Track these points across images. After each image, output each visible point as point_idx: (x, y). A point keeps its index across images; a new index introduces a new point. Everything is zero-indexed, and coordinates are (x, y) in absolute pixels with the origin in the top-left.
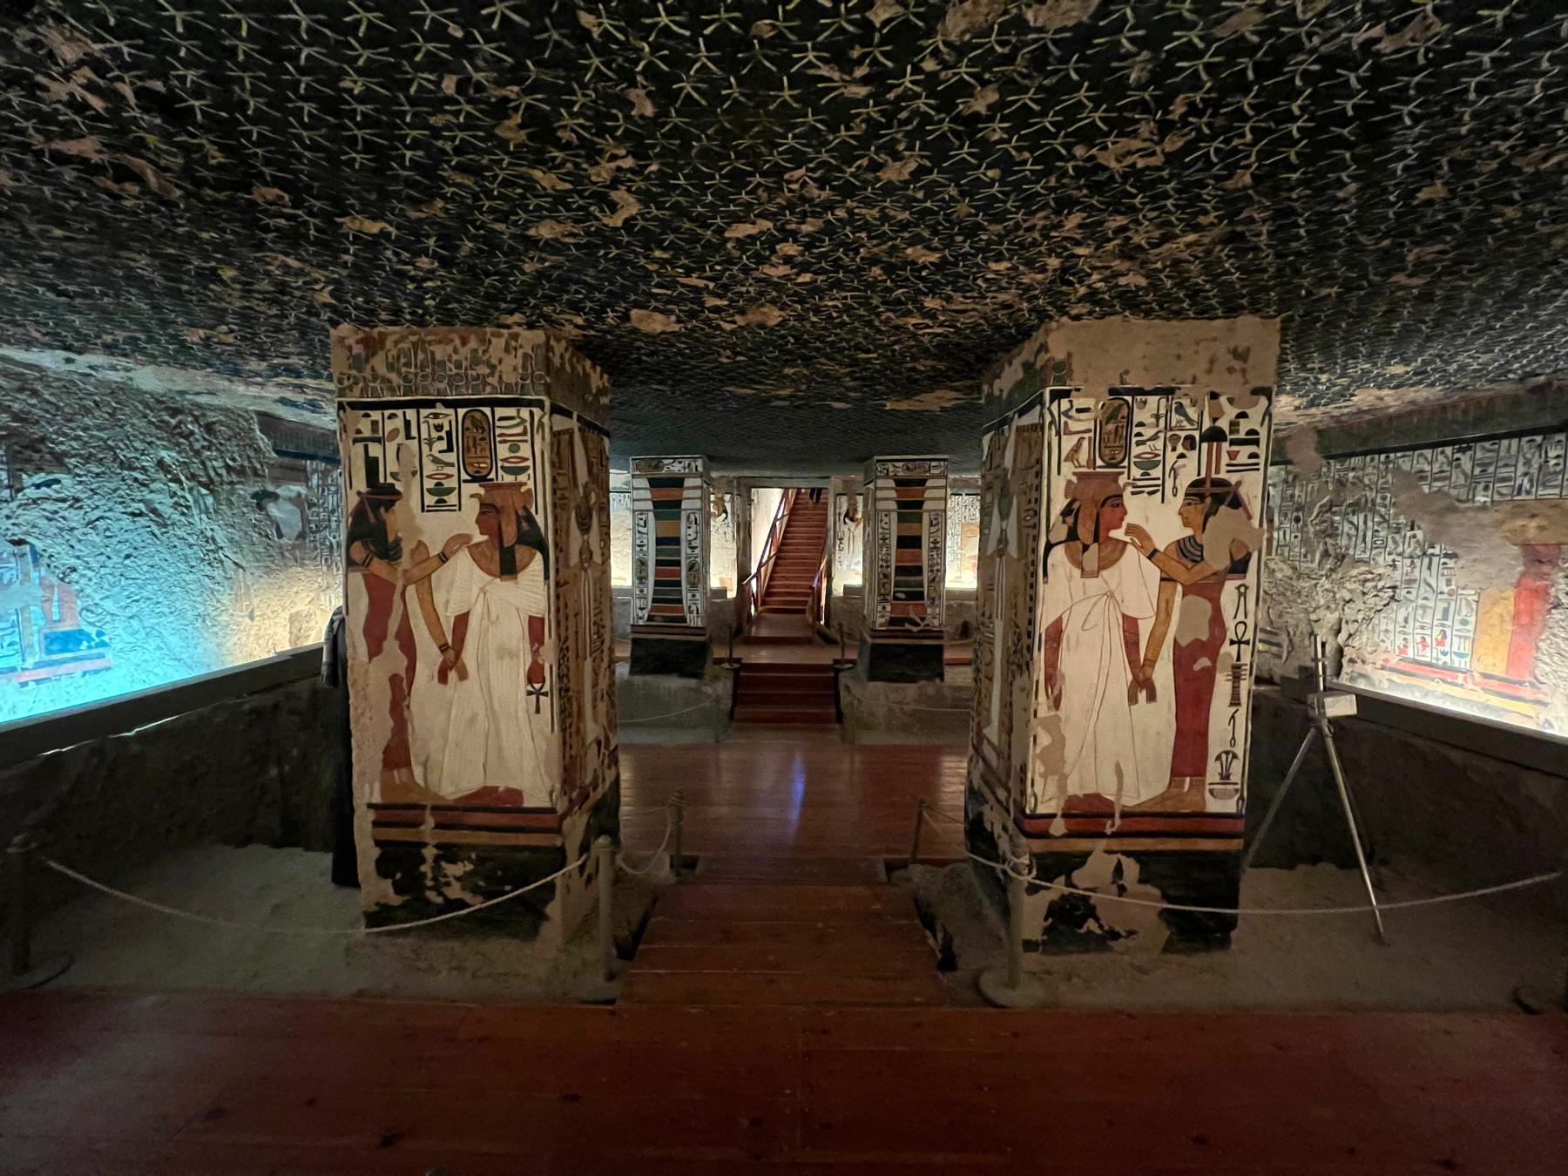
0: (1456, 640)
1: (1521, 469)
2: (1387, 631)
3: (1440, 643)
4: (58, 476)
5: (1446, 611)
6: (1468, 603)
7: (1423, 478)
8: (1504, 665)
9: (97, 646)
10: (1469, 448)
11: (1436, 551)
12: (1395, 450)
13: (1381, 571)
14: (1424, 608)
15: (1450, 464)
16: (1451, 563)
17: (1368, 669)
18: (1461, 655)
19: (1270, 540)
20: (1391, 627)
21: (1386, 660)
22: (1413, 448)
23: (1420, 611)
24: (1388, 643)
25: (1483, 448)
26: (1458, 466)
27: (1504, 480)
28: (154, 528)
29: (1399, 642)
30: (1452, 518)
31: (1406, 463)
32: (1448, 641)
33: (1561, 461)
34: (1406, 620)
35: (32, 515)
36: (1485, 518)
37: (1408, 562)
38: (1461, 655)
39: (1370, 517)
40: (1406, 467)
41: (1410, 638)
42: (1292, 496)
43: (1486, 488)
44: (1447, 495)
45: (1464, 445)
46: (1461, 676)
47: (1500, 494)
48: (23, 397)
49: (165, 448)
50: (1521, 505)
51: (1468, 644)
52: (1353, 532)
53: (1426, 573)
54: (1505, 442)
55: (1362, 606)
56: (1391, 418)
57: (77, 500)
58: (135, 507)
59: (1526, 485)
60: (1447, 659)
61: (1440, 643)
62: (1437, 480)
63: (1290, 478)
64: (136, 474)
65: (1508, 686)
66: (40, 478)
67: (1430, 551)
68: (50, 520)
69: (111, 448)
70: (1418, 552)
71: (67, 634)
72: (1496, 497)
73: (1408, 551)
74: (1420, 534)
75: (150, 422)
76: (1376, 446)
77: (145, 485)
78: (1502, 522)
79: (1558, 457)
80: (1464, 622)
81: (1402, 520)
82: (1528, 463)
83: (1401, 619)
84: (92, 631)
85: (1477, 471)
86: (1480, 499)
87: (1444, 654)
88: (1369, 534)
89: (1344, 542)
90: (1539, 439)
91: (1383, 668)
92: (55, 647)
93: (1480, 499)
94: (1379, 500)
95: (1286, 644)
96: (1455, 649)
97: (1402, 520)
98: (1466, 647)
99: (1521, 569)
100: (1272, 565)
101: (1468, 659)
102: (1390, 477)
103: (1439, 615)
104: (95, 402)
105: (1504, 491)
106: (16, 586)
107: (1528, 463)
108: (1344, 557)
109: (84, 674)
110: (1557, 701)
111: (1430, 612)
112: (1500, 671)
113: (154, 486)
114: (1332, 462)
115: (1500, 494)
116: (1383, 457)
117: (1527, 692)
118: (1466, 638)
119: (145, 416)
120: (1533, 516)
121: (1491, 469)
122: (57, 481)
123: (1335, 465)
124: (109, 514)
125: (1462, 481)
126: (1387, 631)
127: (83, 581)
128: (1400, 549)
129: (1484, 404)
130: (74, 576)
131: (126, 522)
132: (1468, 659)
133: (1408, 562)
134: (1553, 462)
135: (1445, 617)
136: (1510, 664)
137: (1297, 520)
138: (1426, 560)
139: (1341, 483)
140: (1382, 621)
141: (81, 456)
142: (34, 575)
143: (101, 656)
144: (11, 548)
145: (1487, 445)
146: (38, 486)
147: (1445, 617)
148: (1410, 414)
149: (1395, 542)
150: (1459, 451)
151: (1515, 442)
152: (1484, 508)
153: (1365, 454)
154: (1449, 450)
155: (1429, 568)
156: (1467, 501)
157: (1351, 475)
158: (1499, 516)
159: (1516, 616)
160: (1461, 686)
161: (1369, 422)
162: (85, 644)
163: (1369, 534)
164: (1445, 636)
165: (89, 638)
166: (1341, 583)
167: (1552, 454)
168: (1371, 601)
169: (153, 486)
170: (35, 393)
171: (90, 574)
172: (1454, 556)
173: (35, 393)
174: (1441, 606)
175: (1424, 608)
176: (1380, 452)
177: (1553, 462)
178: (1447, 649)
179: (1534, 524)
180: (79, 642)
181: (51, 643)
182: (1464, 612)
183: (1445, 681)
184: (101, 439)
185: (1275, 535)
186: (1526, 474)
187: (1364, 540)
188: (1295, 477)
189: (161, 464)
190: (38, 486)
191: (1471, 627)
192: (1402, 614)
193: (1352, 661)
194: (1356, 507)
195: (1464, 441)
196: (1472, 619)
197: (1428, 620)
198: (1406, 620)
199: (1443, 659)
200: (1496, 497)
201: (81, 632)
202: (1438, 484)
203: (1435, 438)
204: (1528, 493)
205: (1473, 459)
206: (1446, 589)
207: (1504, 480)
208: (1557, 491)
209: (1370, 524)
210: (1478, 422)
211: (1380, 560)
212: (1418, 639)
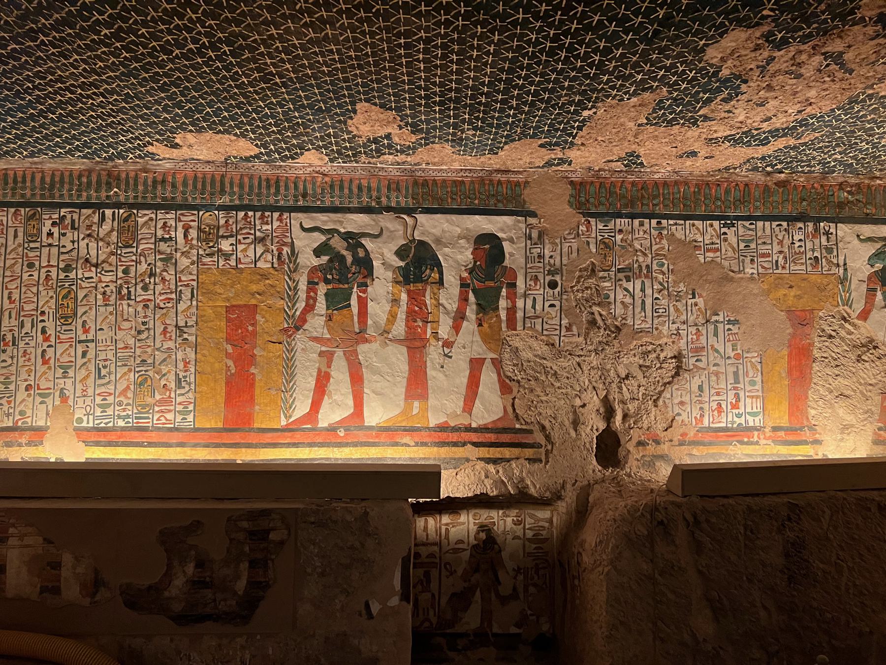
0: (748, 400)
2: (682, 403)
3: (735, 406)
5: (736, 374)
6: (753, 366)
7: (697, 248)
8: (787, 417)
12: (668, 217)
13: (663, 341)
14: (717, 374)
15: (719, 237)
16: (735, 329)
17: (665, 448)
19: (512, 311)
20: (686, 399)
21: (684, 435)
22: (686, 218)
23: (714, 378)
24: (684, 416)
25: (744, 226)
26: (726, 240)
27: (763, 255)
29: (696, 413)
30: (728, 288)
31: (680, 230)
32: (741, 404)
33: (802, 244)
34: (700, 388)
36: (755, 288)
37: (693, 330)
39: (648, 283)
40: (680, 235)
41: (706, 406)
42: (541, 256)
43: (752, 260)
45: (728, 221)
46: (756, 433)
47: (763, 267)
50: (780, 277)
51: (759, 403)
52: (628, 300)
53: (712, 340)
54: (760, 224)
55: (643, 382)
56: (656, 183)
59: (781, 261)
61: (735, 406)
62: (709, 250)
63: (535, 234)
65: (792, 433)
67: (714, 318)
70: (701, 320)
73: (691, 319)
74: (700, 301)
76: (646, 209)
78: (769, 291)
79: (800, 240)
80: (753, 383)
81: (682, 287)
82: (781, 243)
83: (695, 388)
85: (742, 245)
86: (749, 270)
87: (739, 416)
88: (649, 302)
89: (620, 311)
90: (785, 224)
91: (681, 444)
93: (749, 270)
94: (655, 267)
95: (543, 441)
96: (749, 410)
97: (682, 287)
98: (757, 406)
99: (790, 331)
100: (516, 343)
101: (761, 417)
102: (664, 242)
105: (765, 265)
107: (781, 243)
108: (618, 329)
110: (826, 438)
111: (722, 377)
112: (784, 422)
114: (593, 221)
115: (763, 267)
116: (654, 222)
117: (807, 435)
118: (757, 397)
120: (791, 287)
121: (753, 246)
123: (597, 225)
125: (730, 253)
126: (682, 403)
128: (684, 317)
129: (742, 187)
132: (761, 417)
133: (693, 330)
134: (797, 244)
135: (737, 381)
136: (791, 415)
137: (553, 285)
138: (711, 327)
139: (606, 246)
140: (674, 395)
145: (747, 224)
147: (737, 381)
148: (676, 183)
149: (677, 310)
151: (767, 224)
152: (752, 279)
153: (632, 216)
154: (716, 224)
155: (716, 334)
156: (740, 272)
157: (619, 237)
159: (790, 372)
160: (757, 443)
161: (633, 184)
163: (649, 302)
166: (617, 356)
167: (796, 238)
168: (655, 374)
172: (735, 322)
175: (717, 374)
176: (650, 216)
177: (797, 244)
178: (742, 410)
179: (793, 292)
182: (751, 374)
183: (742, 443)
185: (520, 303)
186: (780, 252)
187: (643, 309)
188: (541, 235)
191: (758, 386)
192: (696, 382)
193: (640, 444)
194: (628, 273)
196: (758, 379)
197: (723, 386)
198: (700, 388)
203: (701, 211)
204: (783, 268)
205: (737, 234)
206: (732, 355)
207: (763, 255)
208: (804, 267)
209: (649, 291)
210: (741, 201)
211: (665, 330)
212: (714, 405)
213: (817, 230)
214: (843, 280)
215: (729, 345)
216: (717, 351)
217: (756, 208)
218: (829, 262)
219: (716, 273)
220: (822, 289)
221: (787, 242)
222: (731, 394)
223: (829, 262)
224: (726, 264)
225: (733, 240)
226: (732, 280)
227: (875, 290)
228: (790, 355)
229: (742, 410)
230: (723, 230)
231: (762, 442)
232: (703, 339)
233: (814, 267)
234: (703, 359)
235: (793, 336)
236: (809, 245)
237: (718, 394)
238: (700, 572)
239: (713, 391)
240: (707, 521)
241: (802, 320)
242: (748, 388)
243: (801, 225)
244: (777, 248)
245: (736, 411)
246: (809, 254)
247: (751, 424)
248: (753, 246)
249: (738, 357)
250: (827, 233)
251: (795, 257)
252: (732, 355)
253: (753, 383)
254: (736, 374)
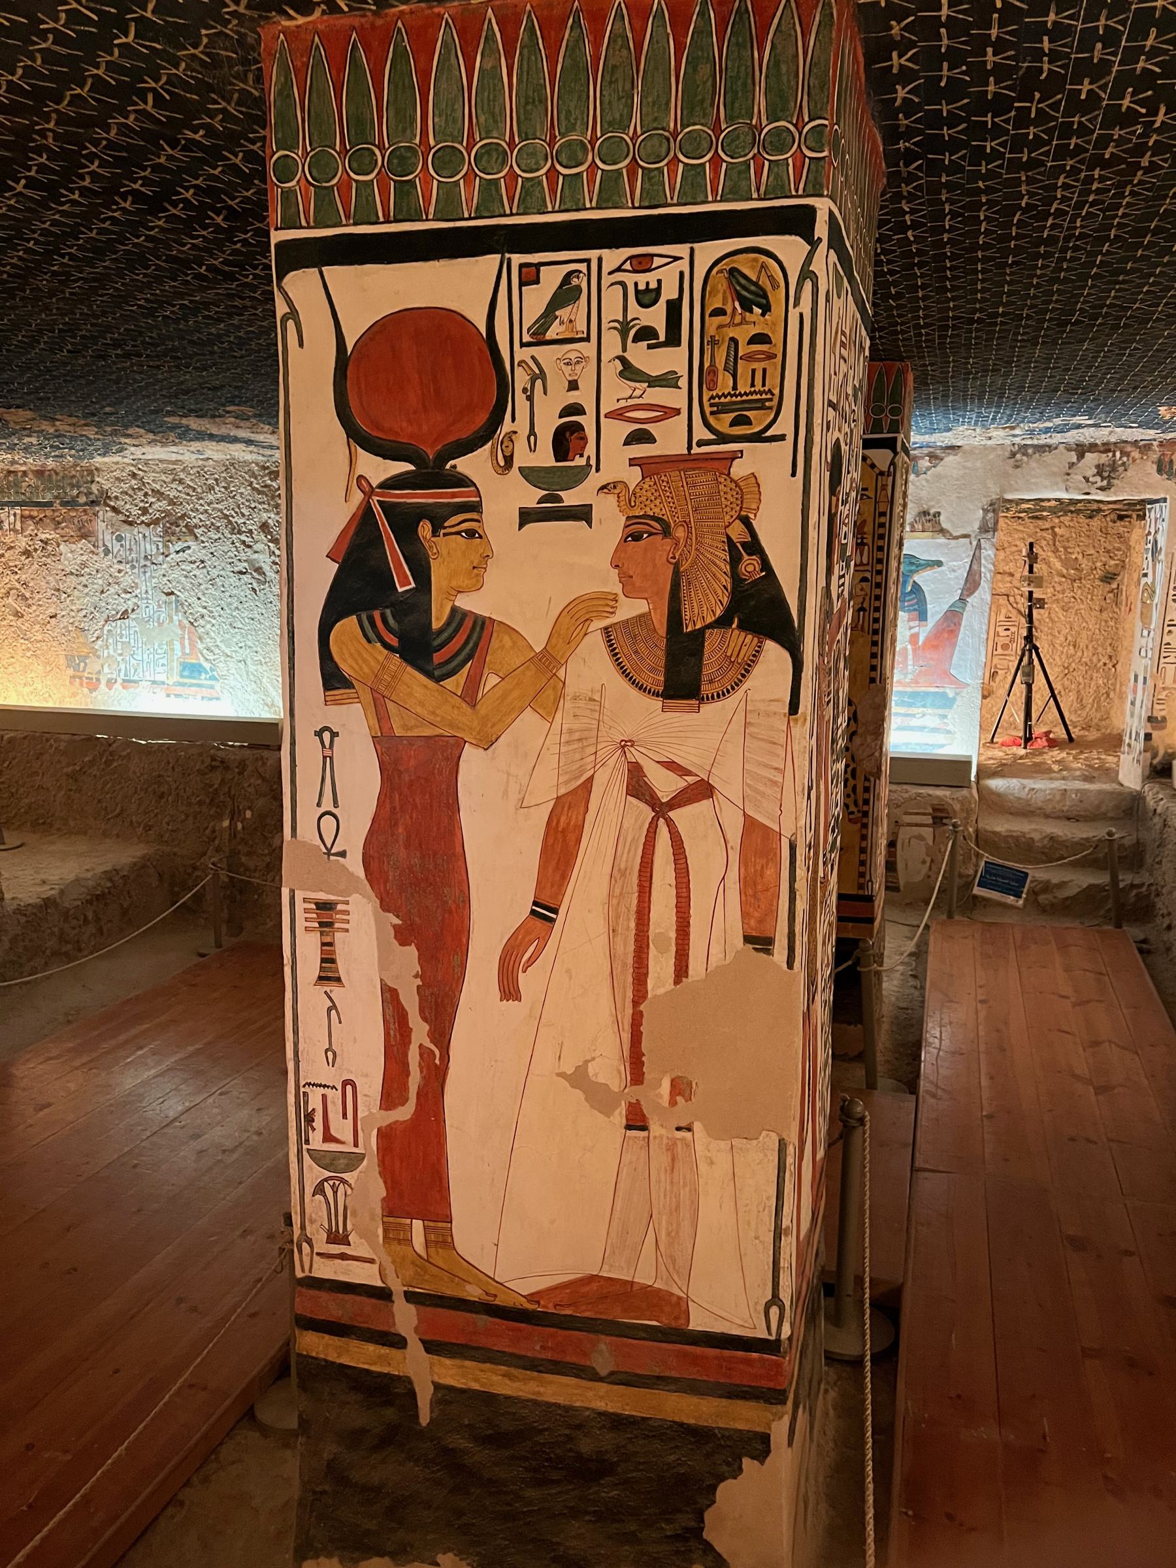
4: (190, 543)
9: (210, 679)
28: (255, 585)
35: (176, 574)
48: (173, 486)
49: (267, 511)
57: (202, 562)
58: (241, 566)
64: (243, 537)
66: (179, 545)
68: (186, 577)
69: (226, 517)
71: (193, 665)
75: (254, 489)
77: (249, 547)
84: (207, 666)
92: (186, 673)
104: (216, 480)
106: (166, 624)
109: (203, 698)
113: (257, 547)
119: (251, 484)
122: (189, 547)
124: (222, 573)
127: (209, 626)
130: (201, 622)
131: (233, 579)
141: (205, 526)
142: (175, 618)
143: (212, 687)
144: (164, 597)
146: (178, 552)
162: (203, 676)
165: (206, 673)
169: (255, 547)
170: (181, 482)
171: (214, 622)
173: (181, 482)
180: (200, 673)
181: (184, 669)
184: (221, 511)
189: (264, 527)
190: (178, 552)
201: (200, 665)
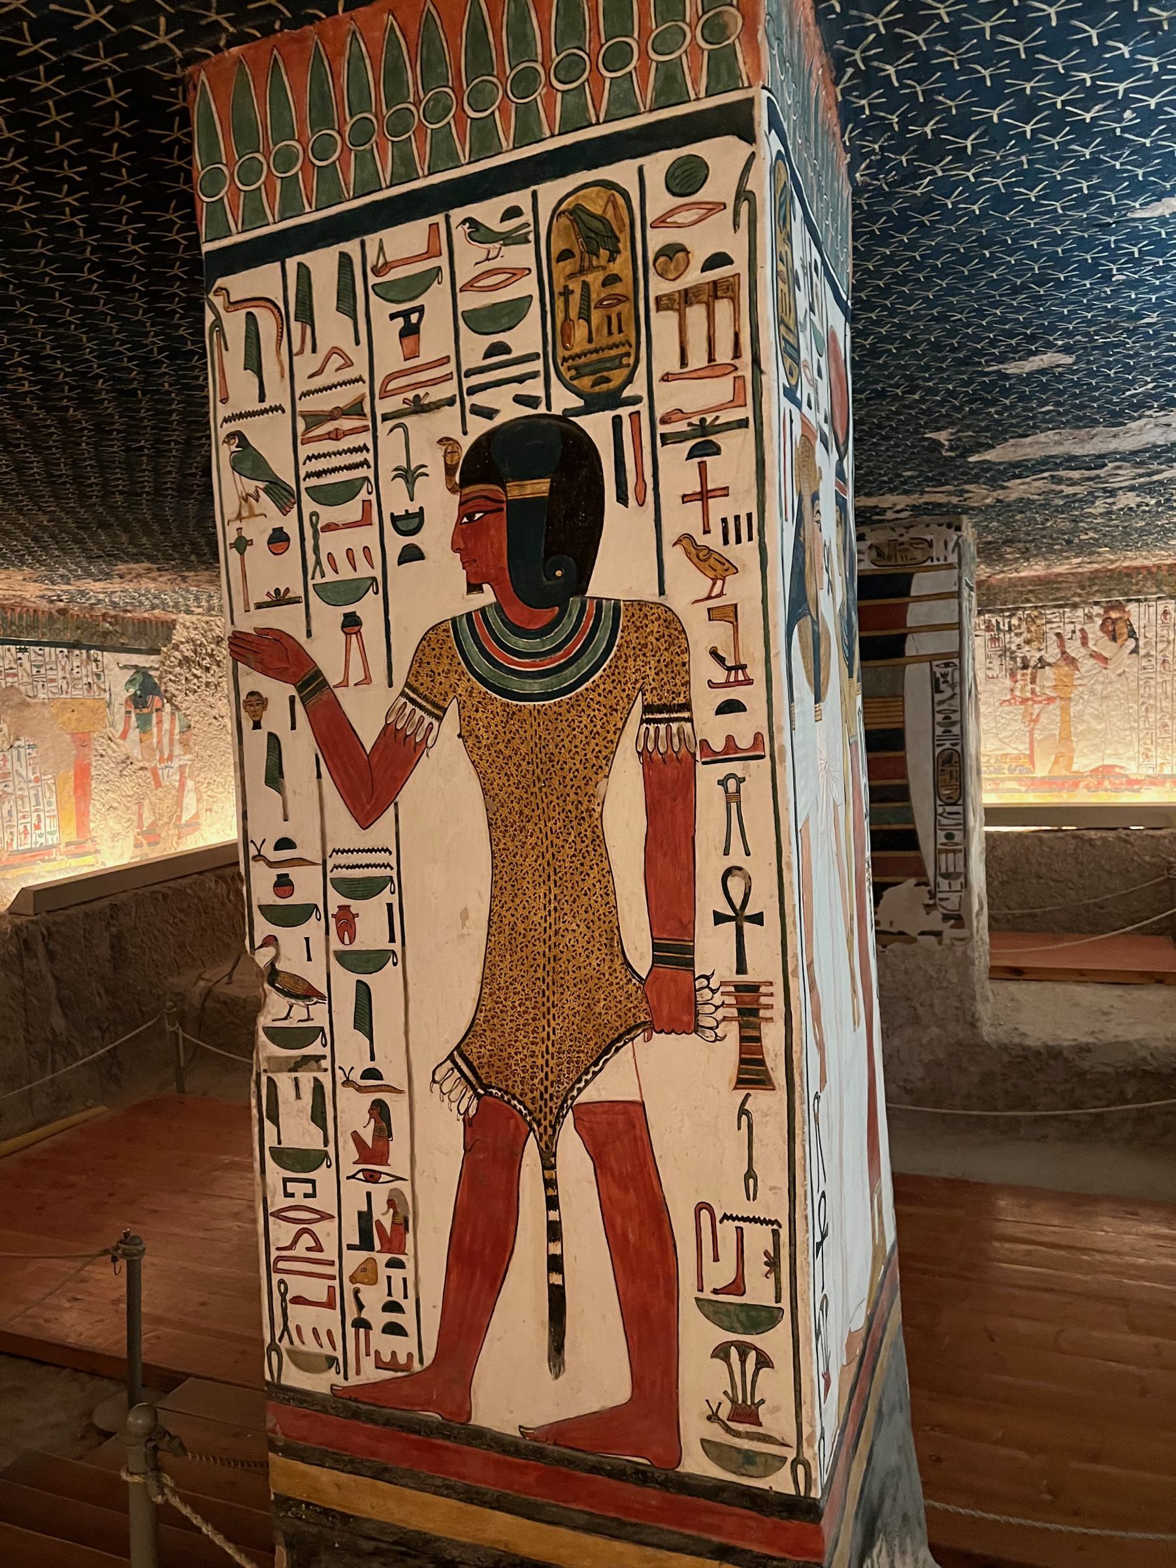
1: (61, 674)
3: (37, 827)
5: (36, 796)
6: (49, 787)
10: (26, 650)
11: (21, 743)
14: (22, 797)
18: (52, 833)
23: (20, 802)
26: (21, 665)
30: (27, 713)
32: (42, 824)
38: (52, 833)
44: (18, 690)
45: (23, 646)
53: (17, 765)
54: (47, 649)
60: (42, 840)
67: (17, 743)
72: (51, 696)
82: (63, 668)
85: (34, 670)
86: (41, 696)
87: (40, 836)
90: (65, 650)
96: (48, 829)
99: (74, 752)
103: (33, 803)
105: (54, 690)
107: (63, 668)
111: (26, 800)
125: (26, 679)
135: (38, 804)
138: (15, 752)
145: (37, 649)
147: (38, 804)
150: (20, 650)
155: (19, 760)
156: (35, 697)
158: (54, 710)
160: (55, 859)
164: (39, 821)
174: (32, 792)
177: (76, 670)
179: (75, 716)
182: (48, 795)
191: (54, 807)
195: (20, 643)
196: (53, 800)
197: (27, 809)
199: (42, 840)
200: (51, 696)
202: (9, 679)
205: (29, 660)
213: (88, 657)
214: (109, 705)
215: (30, 768)
216: (20, 775)
217: (44, 634)
218: (99, 687)
219: (16, 699)
220: (95, 712)
221: (68, 668)
222: (34, 815)
223: (99, 687)
224: (22, 688)
225: (27, 665)
226: (28, 705)
227: (129, 712)
228: (75, 775)
229: (43, 830)
230: (20, 655)
231: (59, 858)
232: (9, 765)
233: (89, 692)
234: (11, 784)
235: (77, 756)
236: (84, 672)
237: (24, 817)
238: (54, 976)
239: (20, 815)
240: (58, 931)
241: (82, 741)
242: (47, 808)
243: (77, 652)
244: (61, 674)
245: (38, 832)
246: (85, 680)
247: (50, 843)
248: (43, 671)
249: (37, 780)
250: (96, 661)
251: (73, 682)
252: (32, 778)
253: (50, 803)
254: (36, 796)
